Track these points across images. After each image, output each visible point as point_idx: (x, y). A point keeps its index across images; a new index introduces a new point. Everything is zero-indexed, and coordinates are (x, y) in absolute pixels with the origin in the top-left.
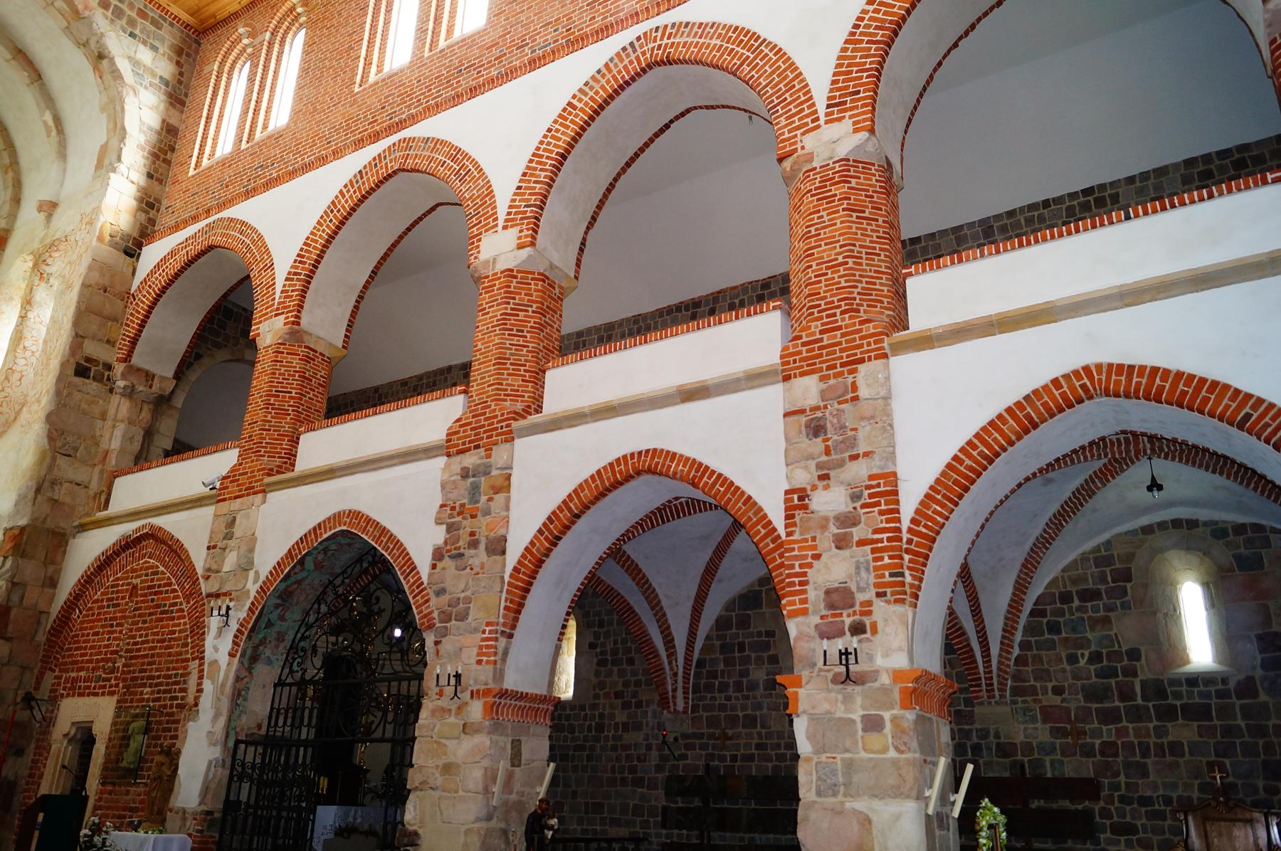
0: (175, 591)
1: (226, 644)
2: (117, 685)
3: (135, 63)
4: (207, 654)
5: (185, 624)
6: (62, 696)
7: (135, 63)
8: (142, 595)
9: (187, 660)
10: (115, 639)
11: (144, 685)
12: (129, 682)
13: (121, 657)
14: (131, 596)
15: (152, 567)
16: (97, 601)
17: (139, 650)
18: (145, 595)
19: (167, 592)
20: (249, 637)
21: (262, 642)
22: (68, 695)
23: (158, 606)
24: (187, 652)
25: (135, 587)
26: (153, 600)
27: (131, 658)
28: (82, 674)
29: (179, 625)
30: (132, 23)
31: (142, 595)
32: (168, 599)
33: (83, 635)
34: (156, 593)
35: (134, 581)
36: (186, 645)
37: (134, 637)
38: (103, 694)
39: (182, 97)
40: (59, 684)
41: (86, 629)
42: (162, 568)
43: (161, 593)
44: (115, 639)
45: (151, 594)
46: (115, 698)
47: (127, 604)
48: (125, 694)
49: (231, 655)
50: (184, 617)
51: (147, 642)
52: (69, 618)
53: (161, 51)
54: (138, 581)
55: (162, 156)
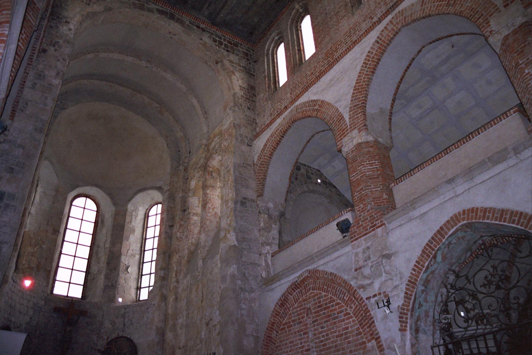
0: (338, 304)
1: (394, 324)
3: (231, 62)
4: (381, 334)
5: (353, 321)
7: (231, 62)
8: (315, 313)
9: (364, 343)
10: (305, 342)
14: (307, 314)
15: (317, 295)
16: (286, 324)
17: (325, 345)
18: (318, 312)
19: (333, 306)
20: (412, 315)
21: (418, 319)
23: (329, 316)
24: (362, 338)
25: (309, 309)
26: (324, 313)
29: (350, 323)
30: (225, 45)
32: (335, 310)
33: (283, 345)
34: (325, 309)
35: (307, 306)
36: (360, 333)
37: (319, 338)
39: (253, 73)
41: (284, 341)
42: (323, 294)
43: (329, 307)
44: (305, 342)
45: (321, 310)
49: (402, 330)
50: (352, 317)
53: (240, 55)
54: (310, 305)
55: (251, 99)
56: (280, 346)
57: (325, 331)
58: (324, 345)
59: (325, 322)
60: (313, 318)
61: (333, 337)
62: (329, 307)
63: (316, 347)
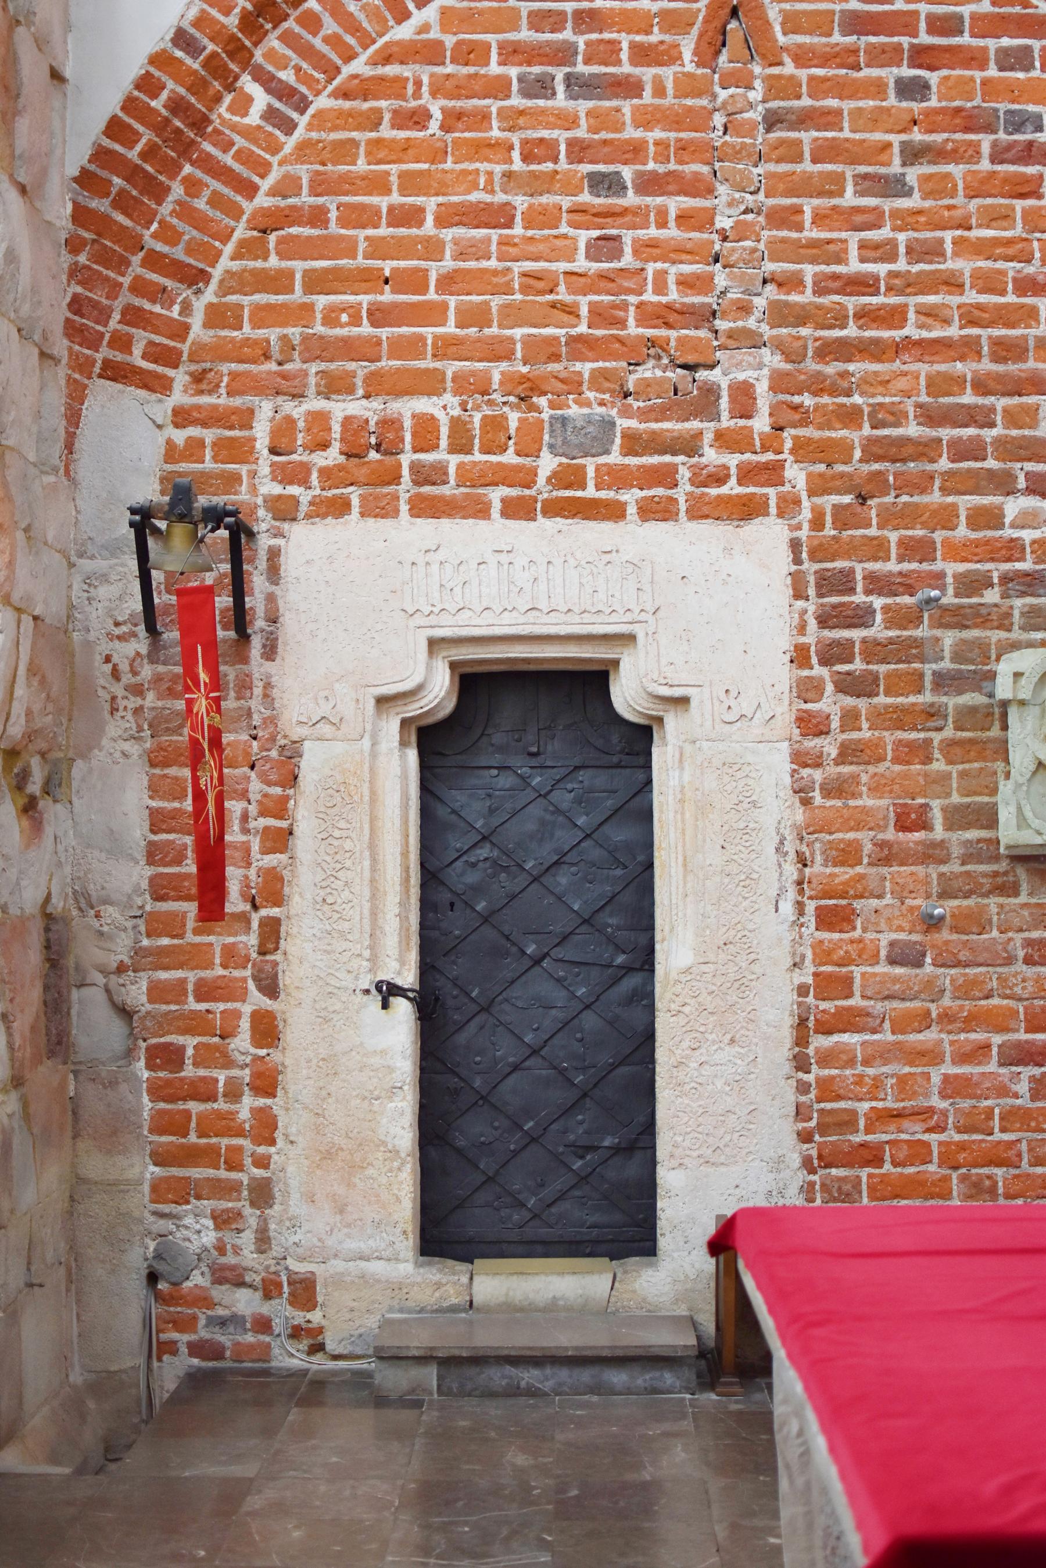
2: (773, 473)
6: (284, 511)
8: (802, 57)
10: (647, 249)
11: (1004, 484)
12: (857, 466)
13: (755, 341)
18: (848, 58)
22: (340, 508)
27: (827, 351)
28: (442, 407)
31: (802, 57)
33: (365, 217)
34: (922, 56)
38: (657, 511)
40: (238, 451)
43: (976, 59)
46: (770, 535)
47: (689, 86)
48: (844, 518)
51: (953, 283)
52: (200, 123)
56: (317, 217)
57: (905, 220)
58: (866, 316)
59: (913, 154)
60: (778, 88)
61: (989, 283)
62: (976, 59)
63: (779, 314)
